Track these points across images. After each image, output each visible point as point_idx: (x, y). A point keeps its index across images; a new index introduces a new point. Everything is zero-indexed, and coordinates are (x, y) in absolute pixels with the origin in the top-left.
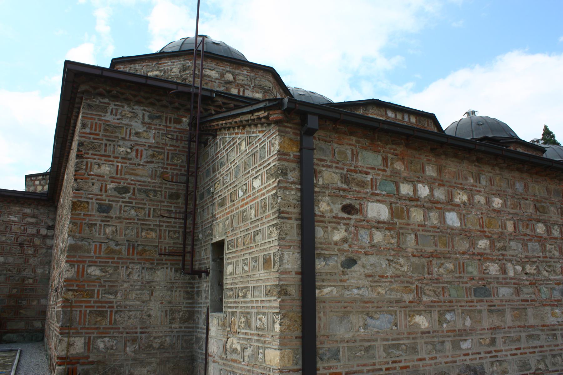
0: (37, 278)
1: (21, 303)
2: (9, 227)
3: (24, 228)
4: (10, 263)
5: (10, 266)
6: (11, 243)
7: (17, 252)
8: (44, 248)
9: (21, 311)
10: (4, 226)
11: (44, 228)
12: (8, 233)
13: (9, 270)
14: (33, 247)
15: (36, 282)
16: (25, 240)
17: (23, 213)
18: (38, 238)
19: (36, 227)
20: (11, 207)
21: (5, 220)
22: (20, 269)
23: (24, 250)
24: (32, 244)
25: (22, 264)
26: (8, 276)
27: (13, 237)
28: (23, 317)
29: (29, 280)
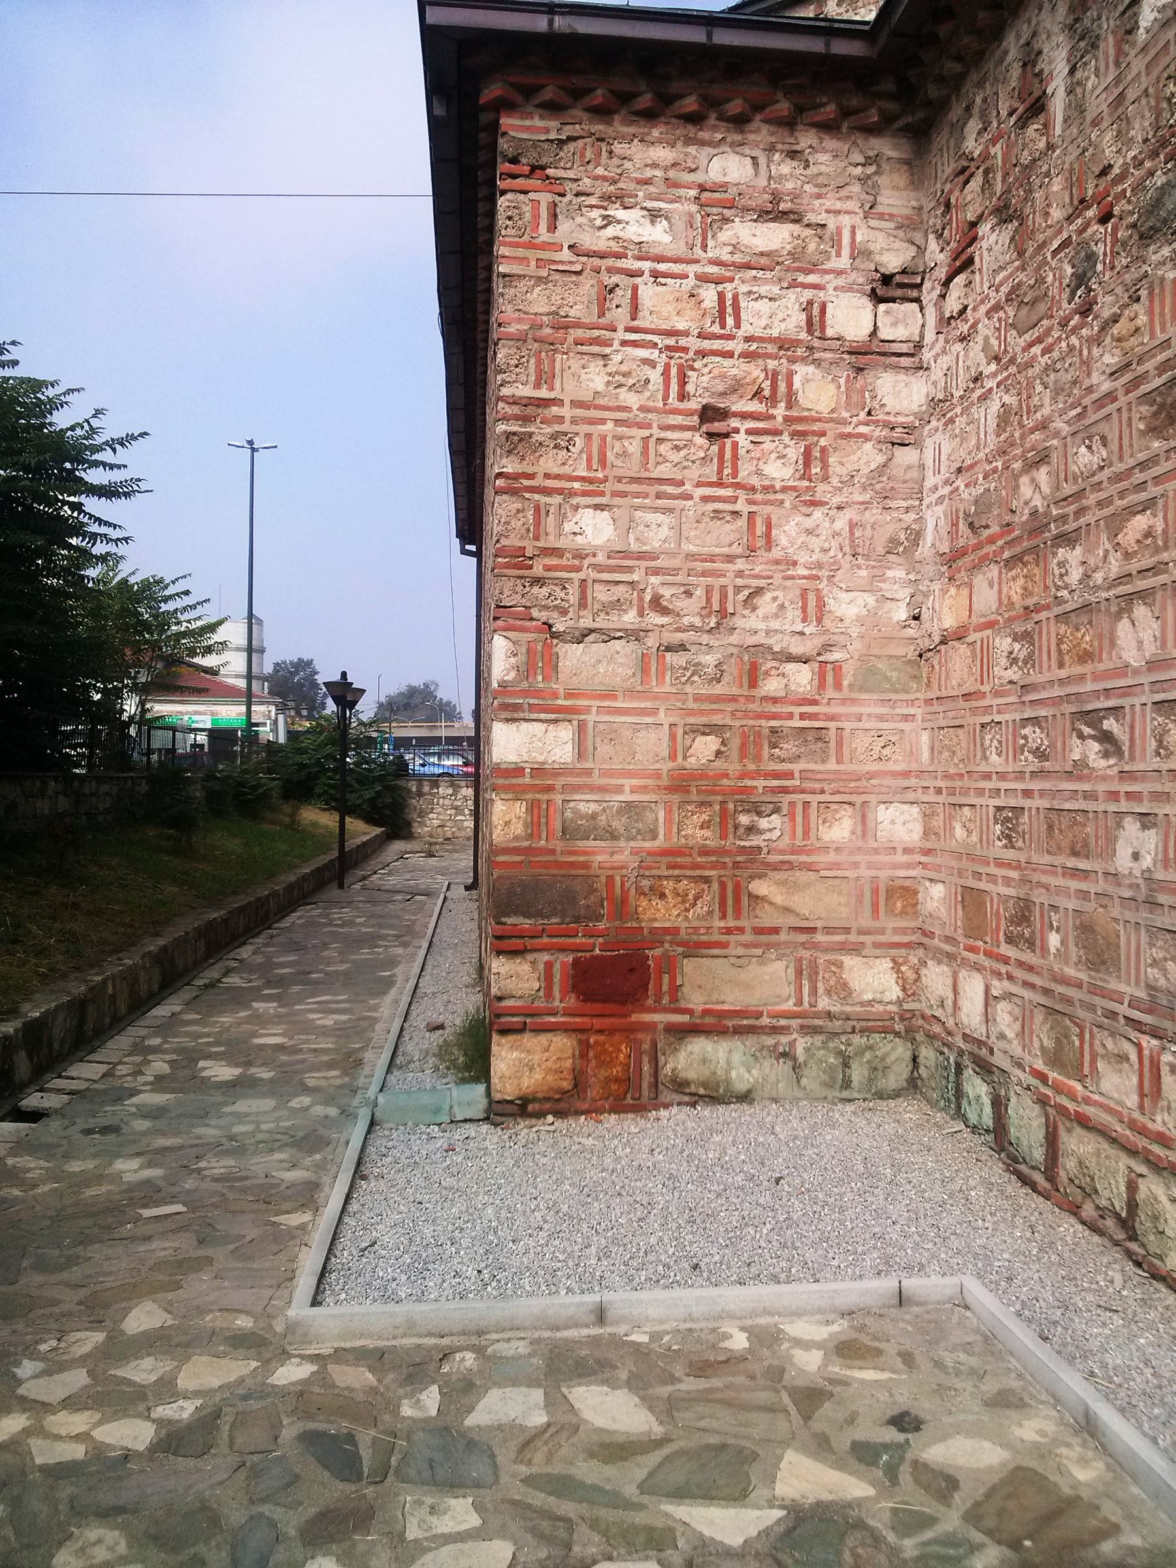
0: (836, 656)
1: (751, 829)
2: (622, 297)
3: (721, 297)
4: (653, 556)
5: (656, 572)
6: (642, 409)
7: (694, 473)
8: (866, 438)
9: (760, 887)
10: (588, 285)
11: (849, 289)
12: (621, 335)
13: (657, 604)
14: (795, 434)
15: (838, 686)
16: (735, 388)
17: (702, 188)
18: (817, 363)
19: (793, 285)
20: (618, 148)
21: (589, 240)
22: (724, 597)
23: (735, 457)
24: (780, 411)
25: (730, 559)
26: (652, 641)
27: (652, 364)
28: (775, 931)
29: (790, 667)
